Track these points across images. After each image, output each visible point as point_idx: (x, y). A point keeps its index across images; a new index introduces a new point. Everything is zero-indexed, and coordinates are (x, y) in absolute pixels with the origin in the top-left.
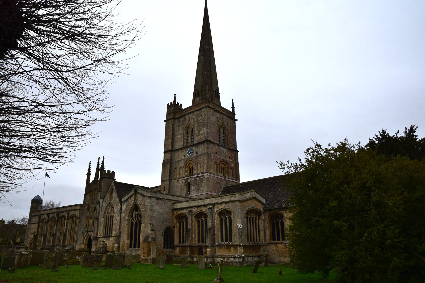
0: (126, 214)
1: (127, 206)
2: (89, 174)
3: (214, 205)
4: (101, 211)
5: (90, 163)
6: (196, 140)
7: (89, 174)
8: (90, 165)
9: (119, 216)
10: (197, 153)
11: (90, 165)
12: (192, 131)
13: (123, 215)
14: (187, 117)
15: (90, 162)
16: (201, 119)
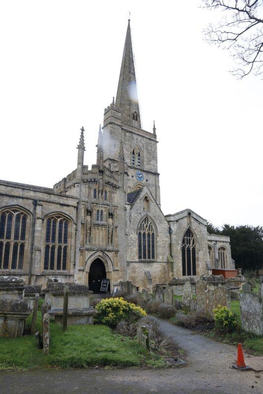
0: (179, 237)
1: (179, 228)
2: (81, 147)
3: (216, 241)
4: (128, 222)
5: (83, 130)
6: (146, 168)
7: (81, 147)
8: (82, 133)
9: (167, 237)
10: (147, 181)
11: (82, 133)
12: (139, 155)
13: (174, 237)
14: (135, 136)
15: (83, 127)
16: (151, 150)
